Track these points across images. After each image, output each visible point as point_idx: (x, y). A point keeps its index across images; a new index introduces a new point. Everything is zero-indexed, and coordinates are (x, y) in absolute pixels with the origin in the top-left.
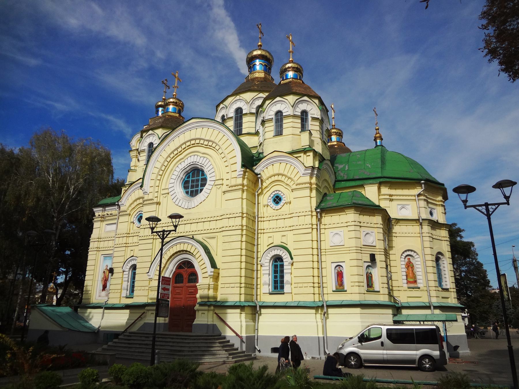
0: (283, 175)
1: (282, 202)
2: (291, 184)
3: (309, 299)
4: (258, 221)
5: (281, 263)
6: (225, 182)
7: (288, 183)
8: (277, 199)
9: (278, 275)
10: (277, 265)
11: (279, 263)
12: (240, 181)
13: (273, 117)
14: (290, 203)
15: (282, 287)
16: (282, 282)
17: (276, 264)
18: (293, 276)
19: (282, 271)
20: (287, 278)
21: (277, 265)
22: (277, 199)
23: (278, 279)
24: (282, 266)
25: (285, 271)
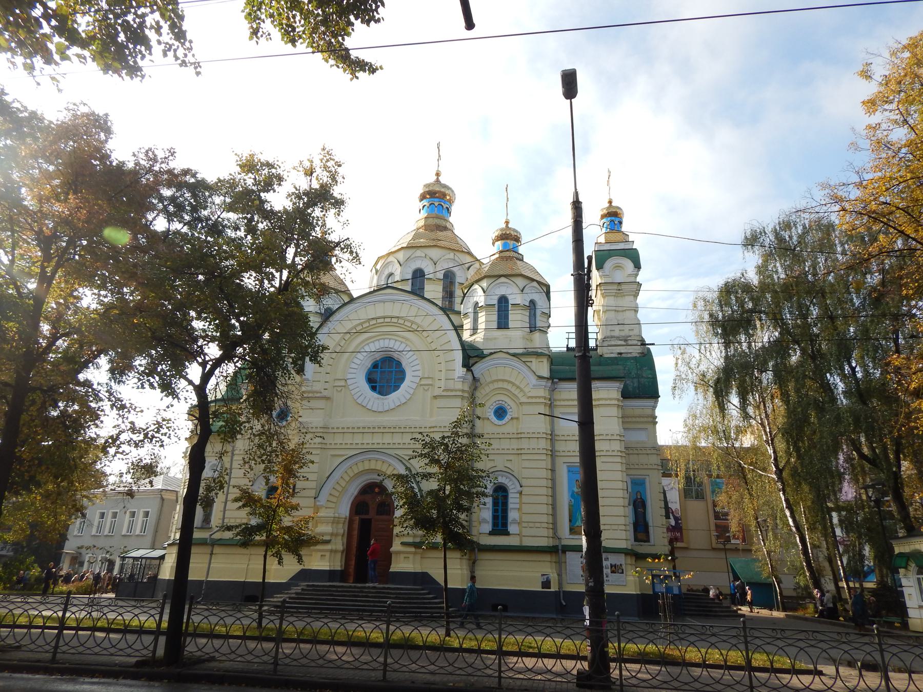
1: (508, 417)
2: (520, 396)
3: (543, 542)
6: (438, 384)
7: (516, 393)
9: (500, 508)
11: (501, 494)
12: (459, 386)
13: (495, 302)
15: (505, 524)
20: (512, 515)
22: (500, 412)
23: (500, 513)
24: (506, 497)
25: (510, 506)
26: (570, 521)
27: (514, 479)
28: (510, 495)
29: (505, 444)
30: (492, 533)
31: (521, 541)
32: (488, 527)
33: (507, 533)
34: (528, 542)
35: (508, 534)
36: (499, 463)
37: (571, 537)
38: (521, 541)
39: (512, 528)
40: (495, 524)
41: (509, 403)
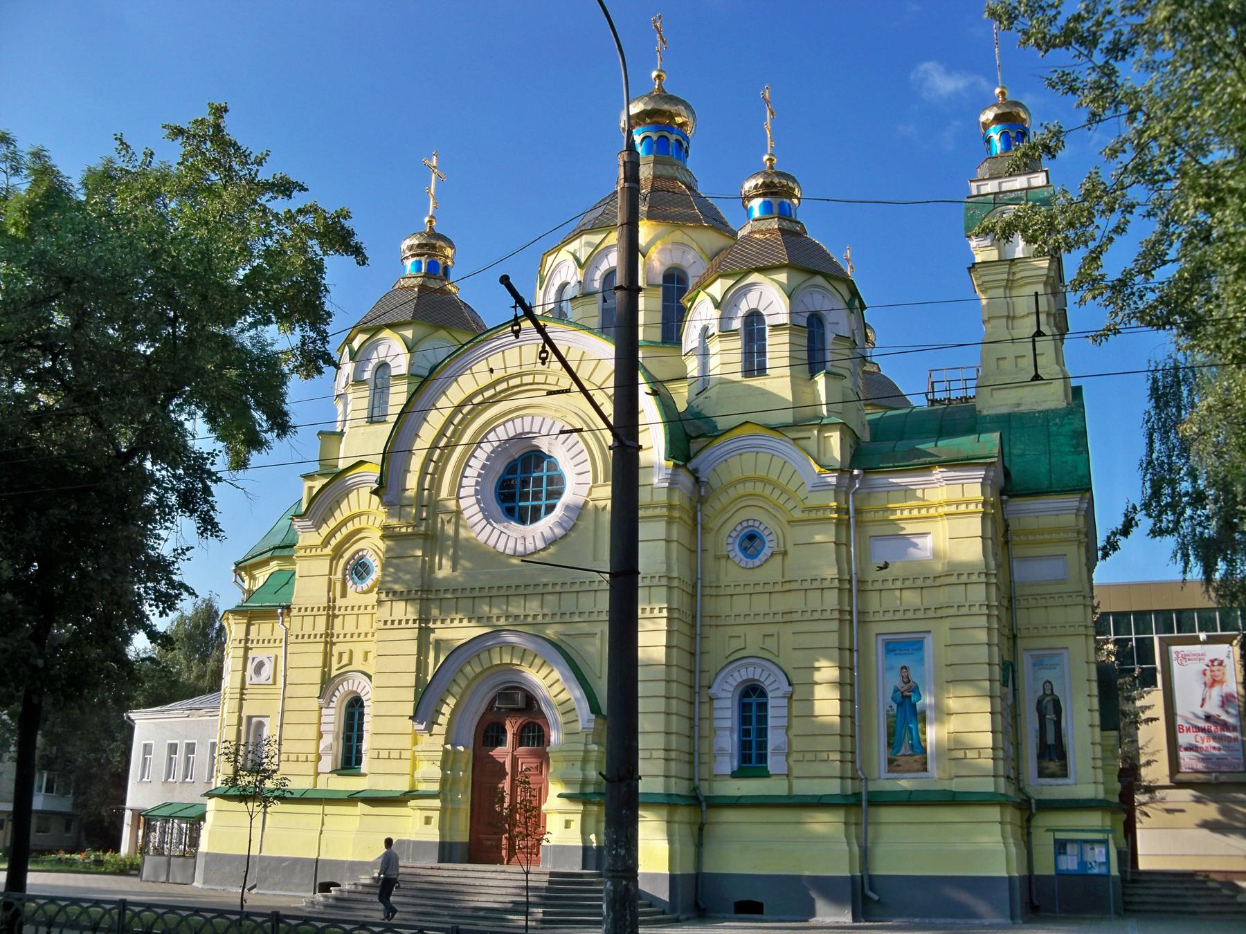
0: (766, 481)
4: (702, 596)
5: (762, 700)
8: (751, 541)
9: (753, 727)
10: (750, 704)
11: (754, 700)
14: (785, 553)
15: (763, 758)
16: (763, 745)
17: (747, 700)
18: (791, 734)
19: (763, 719)
20: (774, 739)
21: (750, 704)
24: (763, 707)
25: (770, 722)
26: (890, 745)
27: (773, 667)
28: (771, 703)
29: (760, 604)
30: (734, 775)
31: (790, 786)
32: (727, 764)
33: (764, 774)
34: (803, 788)
35: (767, 775)
36: (752, 639)
37: (891, 775)
38: (790, 786)
39: (772, 764)
40: (745, 758)
41: (768, 524)
